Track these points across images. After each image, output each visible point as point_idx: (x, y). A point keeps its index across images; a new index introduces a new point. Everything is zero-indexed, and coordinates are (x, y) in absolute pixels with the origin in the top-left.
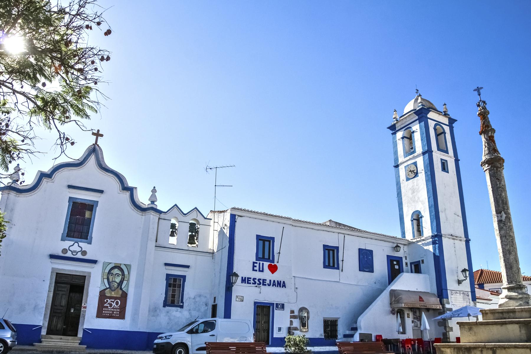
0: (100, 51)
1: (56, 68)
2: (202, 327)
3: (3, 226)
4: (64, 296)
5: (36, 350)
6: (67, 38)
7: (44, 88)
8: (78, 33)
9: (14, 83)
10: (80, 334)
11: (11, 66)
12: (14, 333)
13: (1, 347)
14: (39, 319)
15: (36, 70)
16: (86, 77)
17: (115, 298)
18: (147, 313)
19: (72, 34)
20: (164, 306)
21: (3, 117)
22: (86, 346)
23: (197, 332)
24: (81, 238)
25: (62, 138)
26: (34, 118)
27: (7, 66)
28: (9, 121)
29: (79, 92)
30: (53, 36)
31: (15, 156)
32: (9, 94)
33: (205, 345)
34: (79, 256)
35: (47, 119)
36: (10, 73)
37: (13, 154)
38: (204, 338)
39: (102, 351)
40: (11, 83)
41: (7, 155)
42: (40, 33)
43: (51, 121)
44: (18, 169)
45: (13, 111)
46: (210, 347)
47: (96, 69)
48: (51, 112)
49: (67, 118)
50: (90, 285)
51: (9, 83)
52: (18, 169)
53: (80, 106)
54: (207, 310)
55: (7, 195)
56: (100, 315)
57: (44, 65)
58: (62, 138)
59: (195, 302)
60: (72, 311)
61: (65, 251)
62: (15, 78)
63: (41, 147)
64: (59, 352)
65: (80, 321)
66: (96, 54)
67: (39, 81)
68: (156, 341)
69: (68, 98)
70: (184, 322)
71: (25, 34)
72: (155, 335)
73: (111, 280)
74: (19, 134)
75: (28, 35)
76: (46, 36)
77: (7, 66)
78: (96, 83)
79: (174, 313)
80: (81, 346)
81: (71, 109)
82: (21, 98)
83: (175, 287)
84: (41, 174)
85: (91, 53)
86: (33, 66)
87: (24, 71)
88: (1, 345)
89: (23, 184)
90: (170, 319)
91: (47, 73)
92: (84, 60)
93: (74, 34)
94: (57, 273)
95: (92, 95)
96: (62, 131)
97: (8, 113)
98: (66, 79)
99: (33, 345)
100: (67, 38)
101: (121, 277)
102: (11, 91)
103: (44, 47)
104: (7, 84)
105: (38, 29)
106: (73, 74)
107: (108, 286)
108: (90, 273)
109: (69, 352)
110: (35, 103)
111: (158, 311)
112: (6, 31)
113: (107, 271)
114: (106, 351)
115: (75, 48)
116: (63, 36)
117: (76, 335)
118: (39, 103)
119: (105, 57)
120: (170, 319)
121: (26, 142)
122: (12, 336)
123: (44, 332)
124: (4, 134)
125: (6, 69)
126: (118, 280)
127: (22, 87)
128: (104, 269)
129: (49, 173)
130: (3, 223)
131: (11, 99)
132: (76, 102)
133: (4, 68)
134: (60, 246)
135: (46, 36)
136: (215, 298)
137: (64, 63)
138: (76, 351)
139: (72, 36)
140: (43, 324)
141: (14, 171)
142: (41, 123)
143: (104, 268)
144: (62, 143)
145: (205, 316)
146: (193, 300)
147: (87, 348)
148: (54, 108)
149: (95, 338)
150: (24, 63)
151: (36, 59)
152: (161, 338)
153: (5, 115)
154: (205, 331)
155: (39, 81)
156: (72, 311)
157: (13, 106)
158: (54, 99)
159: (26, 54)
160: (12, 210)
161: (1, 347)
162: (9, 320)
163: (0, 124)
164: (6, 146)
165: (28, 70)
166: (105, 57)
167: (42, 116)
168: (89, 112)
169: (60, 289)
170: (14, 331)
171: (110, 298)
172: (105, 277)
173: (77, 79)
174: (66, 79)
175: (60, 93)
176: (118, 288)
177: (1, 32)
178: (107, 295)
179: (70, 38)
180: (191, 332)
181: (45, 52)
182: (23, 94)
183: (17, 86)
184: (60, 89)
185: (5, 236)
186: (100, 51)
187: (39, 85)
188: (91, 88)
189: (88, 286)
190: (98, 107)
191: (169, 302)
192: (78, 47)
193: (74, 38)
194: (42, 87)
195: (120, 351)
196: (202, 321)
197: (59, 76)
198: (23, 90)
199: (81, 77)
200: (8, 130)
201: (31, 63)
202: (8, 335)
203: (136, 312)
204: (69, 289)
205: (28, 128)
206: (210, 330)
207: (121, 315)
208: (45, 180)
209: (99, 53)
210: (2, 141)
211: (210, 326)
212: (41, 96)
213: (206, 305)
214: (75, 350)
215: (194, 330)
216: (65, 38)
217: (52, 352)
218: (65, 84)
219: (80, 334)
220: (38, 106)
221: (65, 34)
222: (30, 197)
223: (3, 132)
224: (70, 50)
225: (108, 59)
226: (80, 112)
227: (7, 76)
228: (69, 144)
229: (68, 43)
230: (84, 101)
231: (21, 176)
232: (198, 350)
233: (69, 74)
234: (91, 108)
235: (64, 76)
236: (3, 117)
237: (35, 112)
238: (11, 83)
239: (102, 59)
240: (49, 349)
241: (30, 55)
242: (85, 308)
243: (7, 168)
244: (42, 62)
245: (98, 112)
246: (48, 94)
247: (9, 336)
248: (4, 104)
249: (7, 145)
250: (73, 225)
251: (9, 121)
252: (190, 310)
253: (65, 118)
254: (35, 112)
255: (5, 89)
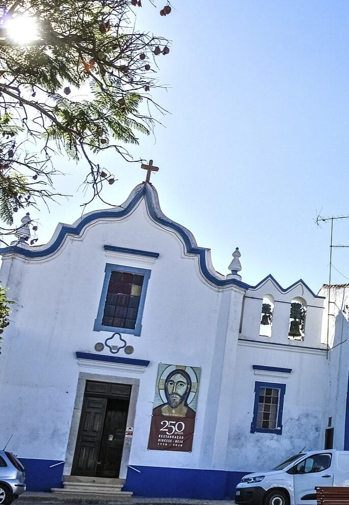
0: (153, 39)
1: (86, 66)
2: (310, 464)
3: (5, 307)
4: (98, 416)
5: (56, 499)
6: (103, 20)
7: (68, 97)
8: (121, 11)
9: (21, 88)
10: (123, 475)
11: (16, 62)
12: (21, 473)
13: (2, 494)
14: (60, 452)
15: (56, 68)
16: (132, 79)
17: (177, 419)
18: (226, 443)
19: (110, 13)
20: (252, 432)
21: (4, 140)
22: (132, 493)
23: (302, 471)
24: (124, 327)
25: (95, 173)
26: (52, 143)
27: (10, 62)
28: (13, 146)
29: (122, 102)
30: (81, 15)
31: (23, 200)
32: (13, 105)
33: (315, 492)
34: (122, 354)
35: (72, 144)
36: (16, 73)
37: (20, 197)
38: (314, 481)
39: (157, 500)
40: (17, 89)
41: (12, 200)
42: (62, 12)
43: (79, 147)
44: (27, 220)
45: (19, 132)
46: (323, 494)
47: (147, 67)
48: (79, 133)
49: (104, 141)
50: (138, 399)
51: (14, 88)
52: (27, 220)
53: (123, 124)
54: (318, 437)
55: (10, 261)
56: (154, 445)
57: (68, 60)
58: (95, 173)
59: (300, 426)
60: (111, 439)
61: (99, 346)
62: (22, 81)
63: (63, 187)
64: (91, 502)
65: (124, 454)
66: (147, 44)
67: (60, 86)
68: (240, 485)
69: (104, 111)
70: (283, 456)
71: (39, 13)
72: (238, 476)
73: (170, 392)
74: (29, 167)
75: (43, 14)
76: (71, 16)
77: (10, 62)
78: (147, 89)
79: (268, 442)
80: (124, 492)
81: (109, 129)
82: (32, 112)
83: (268, 403)
84: (63, 227)
85: (140, 42)
86: (51, 62)
87: (35, 70)
88: (2, 491)
89: (36, 244)
90: (261, 451)
91: (72, 73)
92: (129, 53)
93: (114, 12)
94: (87, 381)
95: (142, 107)
96: (95, 161)
97: (12, 134)
98: (102, 81)
99: (50, 492)
100: (103, 20)
101: (185, 386)
102: (16, 100)
103: (68, 33)
104: (11, 90)
105: (59, 6)
106: (112, 74)
107: (166, 401)
108: (138, 380)
109: (107, 502)
110: (54, 120)
111: (243, 438)
112: (9, 8)
113: (164, 377)
114: (163, 500)
115: (115, 35)
116: (96, 16)
117: (117, 476)
118: (60, 119)
119: (162, 48)
120: (261, 451)
121: (39, 178)
122: (18, 478)
123: (67, 471)
124: (6, 166)
125: (9, 68)
126: (181, 391)
127: (34, 95)
128: (160, 374)
129: (75, 227)
130: (4, 304)
131: (16, 113)
132: (117, 118)
133: (5, 65)
134: (91, 339)
135: (71, 16)
136: (330, 419)
137: (98, 57)
138: (117, 501)
139: (112, 16)
140: (66, 459)
141: (20, 224)
142: (63, 150)
143: (160, 373)
144: (95, 180)
145: (315, 447)
146: (297, 423)
147: (134, 495)
148: (84, 127)
149: (147, 481)
150: (37, 57)
151: (55, 52)
152: (247, 480)
153: (8, 138)
154: (315, 470)
155: (60, 86)
156: (111, 439)
157: (20, 124)
158: (82, 113)
159: (39, 44)
160: (19, 283)
161: (2, 494)
162: (14, 453)
163: (0, 151)
164: (9, 186)
165: (43, 68)
166: (162, 48)
167: (65, 139)
168: (136, 132)
169: (92, 405)
170: (22, 470)
171: (170, 418)
172: (162, 386)
173: (118, 83)
174: (102, 81)
175: (91, 104)
176: (181, 403)
177: (1, 9)
178: (164, 414)
179: (107, 19)
180: (293, 471)
181: (69, 40)
182: (36, 105)
183: (26, 92)
184: (91, 98)
185: (8, 323)
186: (153, 39)
187: (60, 92)
188: (139, 97)
189: (136, 400)
190: (150, 125)
191: (260, 425)
192: (120, 32)
193: (113, 20)
194: (64, 95)
195: (183, 501)
196: (310, 454)
197: (91, 78)
198: (35, 99)
199: (124, 78)
200: (12, 161)
201: (48, 57)
202: (11, 476)
203: (208, 442)
204: (106, 407)
205: (43, 157)
206: (322, 468)
207: (187, 445)
208: (68, 238)
209: (153, 42)
210: (3, 177)
211: (322, 462)
212: (62, 108)
213: (317, 430)
214: (116, 499)
215: (298, 469)
216: (100, 19)
217: (80, 502)
218: (100, 91)
219: (123, 475)
220: (58, 124)
221: (100, 12)
222: (38, 265)
223: (4, 163)
224: (107, 37)
225: (166, 51)
226: (122, 132)
227: (11, 78)
228: (105, 183)
229: (104, 27)
230: (130, 116)
231: (32, 231)
232: (303, 499)
233: (107, 74)
234: (140, 126)
235: (99, 77)
236: (4, 140)
237: (54, 132)
238: (17, 89)
239: (157, 51)
240: (76, 497)
241: (45, 45)
242: (131, 434)
243: (10, 219)
244: (64, 56)
245: (151, 132)
246: (74, 105)
247: (14, 477)
248: (7, 121)
249: (11, 183)
250: (112, 307)
251: (13, 146)
252: (291, 437)
253: (100, 142)
254: (54, 132)
255: (8, 98)
